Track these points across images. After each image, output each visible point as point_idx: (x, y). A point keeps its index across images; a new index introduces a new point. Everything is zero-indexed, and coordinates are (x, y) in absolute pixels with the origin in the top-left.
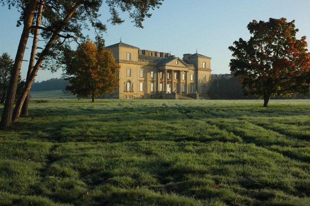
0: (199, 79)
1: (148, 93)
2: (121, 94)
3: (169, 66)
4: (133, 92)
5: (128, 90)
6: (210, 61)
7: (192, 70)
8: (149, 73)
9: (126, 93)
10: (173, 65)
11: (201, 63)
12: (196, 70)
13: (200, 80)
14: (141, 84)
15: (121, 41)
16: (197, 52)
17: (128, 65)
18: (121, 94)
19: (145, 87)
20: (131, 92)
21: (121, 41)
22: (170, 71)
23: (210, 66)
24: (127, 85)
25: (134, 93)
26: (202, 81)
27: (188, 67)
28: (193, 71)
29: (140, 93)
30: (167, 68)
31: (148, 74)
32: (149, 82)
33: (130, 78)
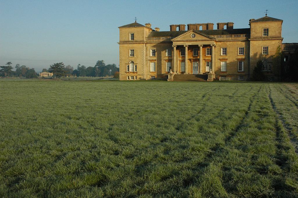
0: (251, 54)
1: (162, 73)
3: (177, 41)
5: (130, 71)
7: (242, 41)
8: (164, 52)
9: (128, 74)
10: (186, 39)
11: (257, 30)
12: (248, 42)
13: (255, 55)
14: (152, 65)
15: (136, 21)
16: (266, 15)
17: (131, 45)
19: (159, 66)
20: (134, 73)
22: (181, 48)
23: (280, 33)
24: (128, 66)
25: (138, 73)
26: (261, 55)
27: (212, 39)
28: (244, 43)
29: (150, 74)
30: (175, 44)
31: (163, 52)
32: (163, 62)
33: (133, 59)
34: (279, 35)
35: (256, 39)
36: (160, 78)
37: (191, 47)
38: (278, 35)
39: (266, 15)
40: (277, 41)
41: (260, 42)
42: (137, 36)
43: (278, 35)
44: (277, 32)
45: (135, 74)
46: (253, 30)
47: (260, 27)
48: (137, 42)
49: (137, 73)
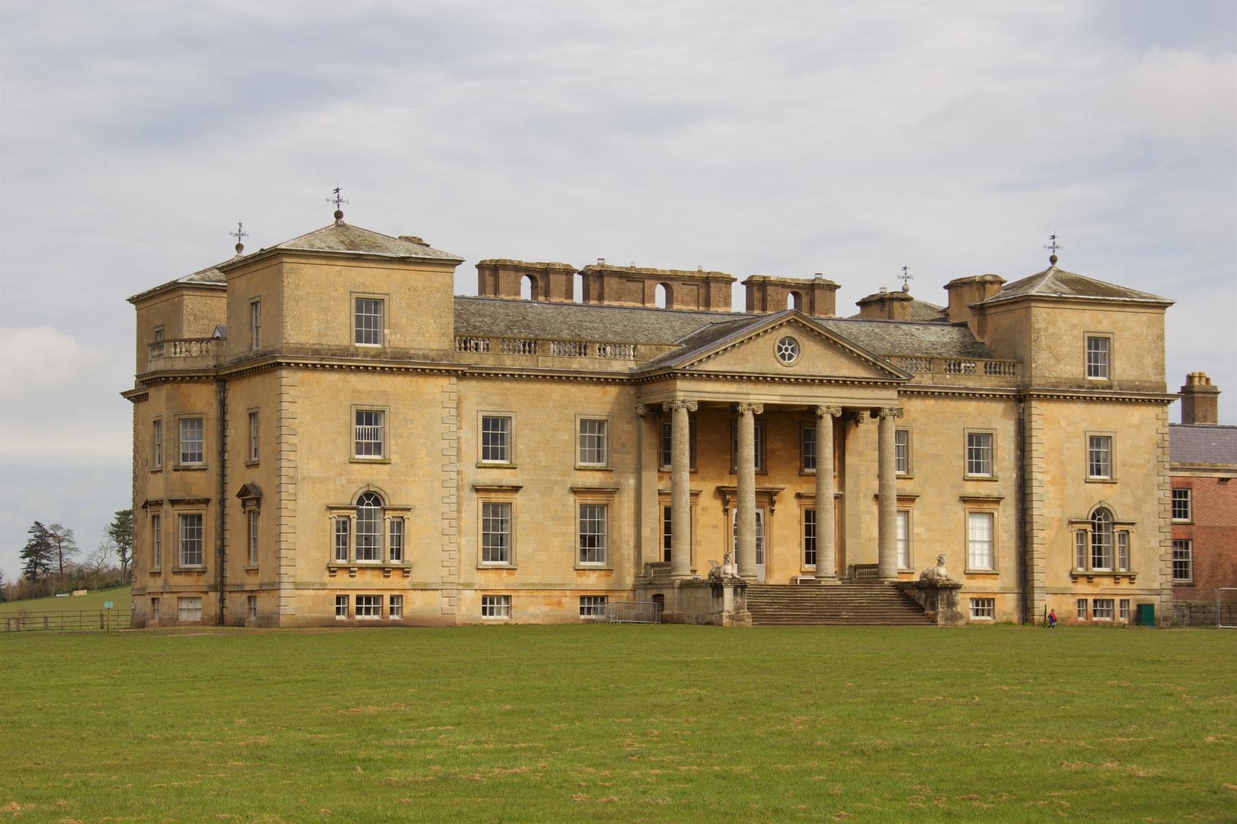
2: (298, 586)
6: (1162, 321)
11: (1058, 345)
15: (338, 215)
16: (1053, 260)
18: (298, 586)
21: (338, 215)
25: (416, 576)
34: (1158, 379)
35: (1055, 395)
36: (547, 608)
37: (771, 417)
38: (1153, 378)
39: (1053, 260)
40: (1151, 412)
41: (1077, 409)
42: (404, 321)
43: (1154, 377)
44: (1148, 361)
45: (395, 581)
46: (1044, 342)
47: (1074, 327)
48: (402, 365)
49: (405, 571)
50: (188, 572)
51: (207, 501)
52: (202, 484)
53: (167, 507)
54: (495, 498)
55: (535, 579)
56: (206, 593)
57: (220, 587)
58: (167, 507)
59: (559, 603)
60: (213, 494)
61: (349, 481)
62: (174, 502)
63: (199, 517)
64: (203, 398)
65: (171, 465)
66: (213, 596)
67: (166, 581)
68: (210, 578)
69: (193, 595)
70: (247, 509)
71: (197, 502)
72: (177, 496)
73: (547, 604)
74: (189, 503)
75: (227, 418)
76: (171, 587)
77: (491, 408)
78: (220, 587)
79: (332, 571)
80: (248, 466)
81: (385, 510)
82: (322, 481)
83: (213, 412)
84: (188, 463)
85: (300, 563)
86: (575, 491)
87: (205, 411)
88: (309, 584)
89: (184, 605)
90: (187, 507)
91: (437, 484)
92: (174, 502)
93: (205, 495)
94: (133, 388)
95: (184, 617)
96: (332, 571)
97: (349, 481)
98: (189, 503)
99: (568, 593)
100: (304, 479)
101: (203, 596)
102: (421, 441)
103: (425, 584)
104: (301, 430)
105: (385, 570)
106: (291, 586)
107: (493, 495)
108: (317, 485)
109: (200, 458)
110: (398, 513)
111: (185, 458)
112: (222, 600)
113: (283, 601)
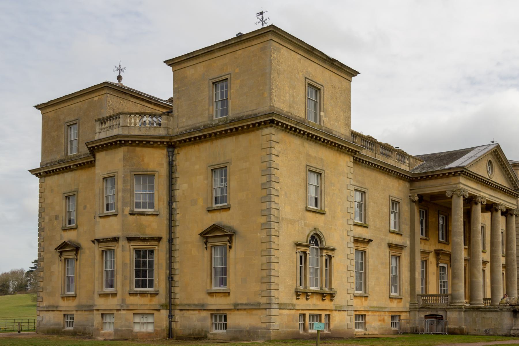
2: (282, 306)
4: (332, 296)
18: (282, 306)
45: (327, 304)
50: (143, 294)
51: (159, 239)
52: (156, 226)
53: (123, 242)
54: (361, 247)
55: (375, 304)
56: (159, 310)
57: (170, 306)
58: (123, 242)
59: (384, 320)
60: (164, 234)
61: (305, 225)
62: (130, 239)
63: (152, 251)
64: (155, 159)
65: (127, 210)
66: (164, 313)
67: (123, 300)
68: (162, 298)
69: (147, 312)
70: (209, 245)
71: (152, 239)
72: (133, 234)
73: (380, 321)
74: (144, 240)
75: (176, 175)
76: (128, 305)
77: (358, 184)
78: (170, 306)
79: (298, 294)
80: (209, 211)
81: (322, 249)
82: (292, 222)
83: (164, 171)
84: (141, 210)
85: (281, 288)
86: (390, 246)
87: (157, 170)
88: (285, 305)
89: (137, 319)
90: (141, 243)
91: (345, 233)
92: (130, 239)
93: (156, 235)
94: (39, 167)
95: (137, 329)
96: (298, 294)
97: (305, 225)
98: (144, 240)
99: (387, 313)
100: (282, 219)
101: (156, 313)
102: (338, 200)
103: (341, 306)
104: (281, 180)
105: (322, 295)
106: (276, 306)
107: (359, 245)
108: (290, 226)
109: (151, 206)
110: (329, 253)
111: (138, 205)
112: (171, 316)
113: (273, 319)
